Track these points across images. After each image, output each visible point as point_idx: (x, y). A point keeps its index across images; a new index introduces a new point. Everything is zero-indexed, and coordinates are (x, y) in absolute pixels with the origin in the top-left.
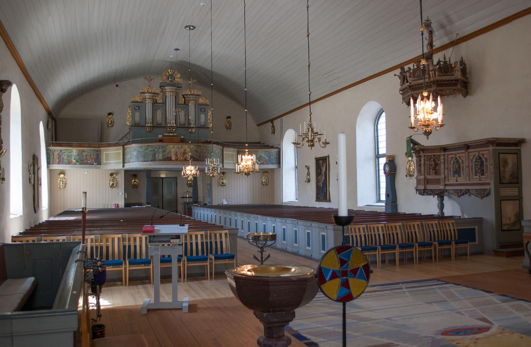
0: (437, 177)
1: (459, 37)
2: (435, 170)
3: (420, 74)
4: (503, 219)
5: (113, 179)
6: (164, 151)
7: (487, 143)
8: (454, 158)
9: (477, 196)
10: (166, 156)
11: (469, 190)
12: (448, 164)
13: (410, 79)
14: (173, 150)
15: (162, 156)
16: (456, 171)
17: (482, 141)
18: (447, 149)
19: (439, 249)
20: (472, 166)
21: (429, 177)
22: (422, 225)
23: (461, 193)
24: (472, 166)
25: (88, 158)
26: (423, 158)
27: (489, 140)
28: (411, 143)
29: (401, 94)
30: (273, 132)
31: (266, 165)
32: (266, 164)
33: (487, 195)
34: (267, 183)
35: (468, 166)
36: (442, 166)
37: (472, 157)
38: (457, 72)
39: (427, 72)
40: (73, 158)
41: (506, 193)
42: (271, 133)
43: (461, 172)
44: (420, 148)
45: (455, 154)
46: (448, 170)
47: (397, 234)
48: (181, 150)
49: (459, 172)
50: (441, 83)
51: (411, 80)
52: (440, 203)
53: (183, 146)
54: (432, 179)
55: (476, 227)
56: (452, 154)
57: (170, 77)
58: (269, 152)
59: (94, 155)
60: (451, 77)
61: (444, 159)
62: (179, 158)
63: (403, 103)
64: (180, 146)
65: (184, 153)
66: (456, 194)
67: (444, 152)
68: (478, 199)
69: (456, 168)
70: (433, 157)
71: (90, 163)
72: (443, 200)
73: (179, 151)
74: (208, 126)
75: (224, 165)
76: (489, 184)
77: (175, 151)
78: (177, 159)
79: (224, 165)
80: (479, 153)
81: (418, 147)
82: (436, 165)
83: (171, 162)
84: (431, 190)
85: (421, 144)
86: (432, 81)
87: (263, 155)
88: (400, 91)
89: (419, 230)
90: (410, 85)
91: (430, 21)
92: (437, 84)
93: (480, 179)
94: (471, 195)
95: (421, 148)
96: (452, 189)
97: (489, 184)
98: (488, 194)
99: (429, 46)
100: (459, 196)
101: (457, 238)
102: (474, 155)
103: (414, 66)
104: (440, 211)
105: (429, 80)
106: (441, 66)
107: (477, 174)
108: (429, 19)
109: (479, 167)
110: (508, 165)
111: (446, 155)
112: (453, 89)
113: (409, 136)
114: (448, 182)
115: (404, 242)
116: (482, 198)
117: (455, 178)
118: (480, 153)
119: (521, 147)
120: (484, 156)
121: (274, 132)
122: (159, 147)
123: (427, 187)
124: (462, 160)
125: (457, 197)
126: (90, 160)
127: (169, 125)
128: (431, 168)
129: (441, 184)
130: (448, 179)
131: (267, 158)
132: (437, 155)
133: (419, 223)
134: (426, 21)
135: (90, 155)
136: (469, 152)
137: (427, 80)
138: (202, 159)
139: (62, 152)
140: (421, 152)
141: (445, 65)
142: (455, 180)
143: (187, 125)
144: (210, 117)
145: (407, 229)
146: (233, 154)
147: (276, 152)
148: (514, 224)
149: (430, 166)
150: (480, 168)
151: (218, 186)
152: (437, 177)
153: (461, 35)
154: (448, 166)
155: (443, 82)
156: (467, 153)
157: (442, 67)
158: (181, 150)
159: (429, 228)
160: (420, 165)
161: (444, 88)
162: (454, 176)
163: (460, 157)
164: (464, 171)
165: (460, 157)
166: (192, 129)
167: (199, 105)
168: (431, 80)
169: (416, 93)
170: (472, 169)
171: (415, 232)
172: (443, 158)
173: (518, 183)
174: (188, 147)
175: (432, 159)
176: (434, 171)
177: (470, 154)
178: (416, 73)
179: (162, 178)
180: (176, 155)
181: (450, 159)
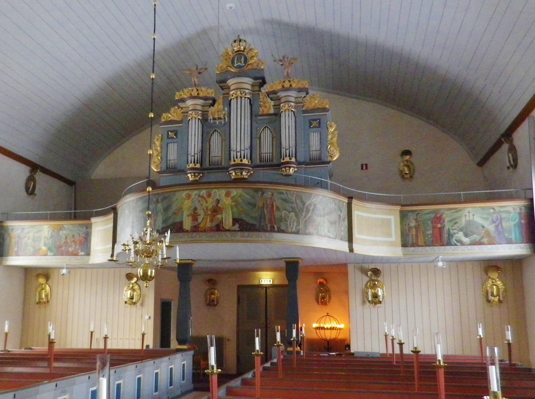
5: (133, 287)
6: (166, 209)
10: (170, 222)
14: (187, 204)
15: (164, 221)
25: (69, 241)
30: (512, 163)
31: (489, 246)
32: (488, 244)
34: (501, 299)
40: (42, 243)
42: (508, 168)
48: (207, 202)
53: (212, 192)
57: (236, 58)
58: (497, 209)
59: (79, 235)
62: (201, 226)
64: (203, 192)
65: (216, 210)
71: (73, 251)
73: (202, 205)
74: (329, 159)
75: (354, 244)
77: (190, 207)
78: (195, 226)
79: (355, 246)
83: (181, 234)
87: (478, 219)
121: (515, 165)
122: (157, 200)
126: (71, 246)
127: (232, 163)
131: (491, 228)
135: (73, 236)
138: (269, 226)
139: (26, 231)
143: (275, 162)
144: (332, 139)
146: (390, 220)
147: (521, 209)
151: (364, 302)
158: (207, 202)
166: (285, 167)
167: (305, 112)
174: (228, 195)
179: (266, 287)
180: (195, 216)
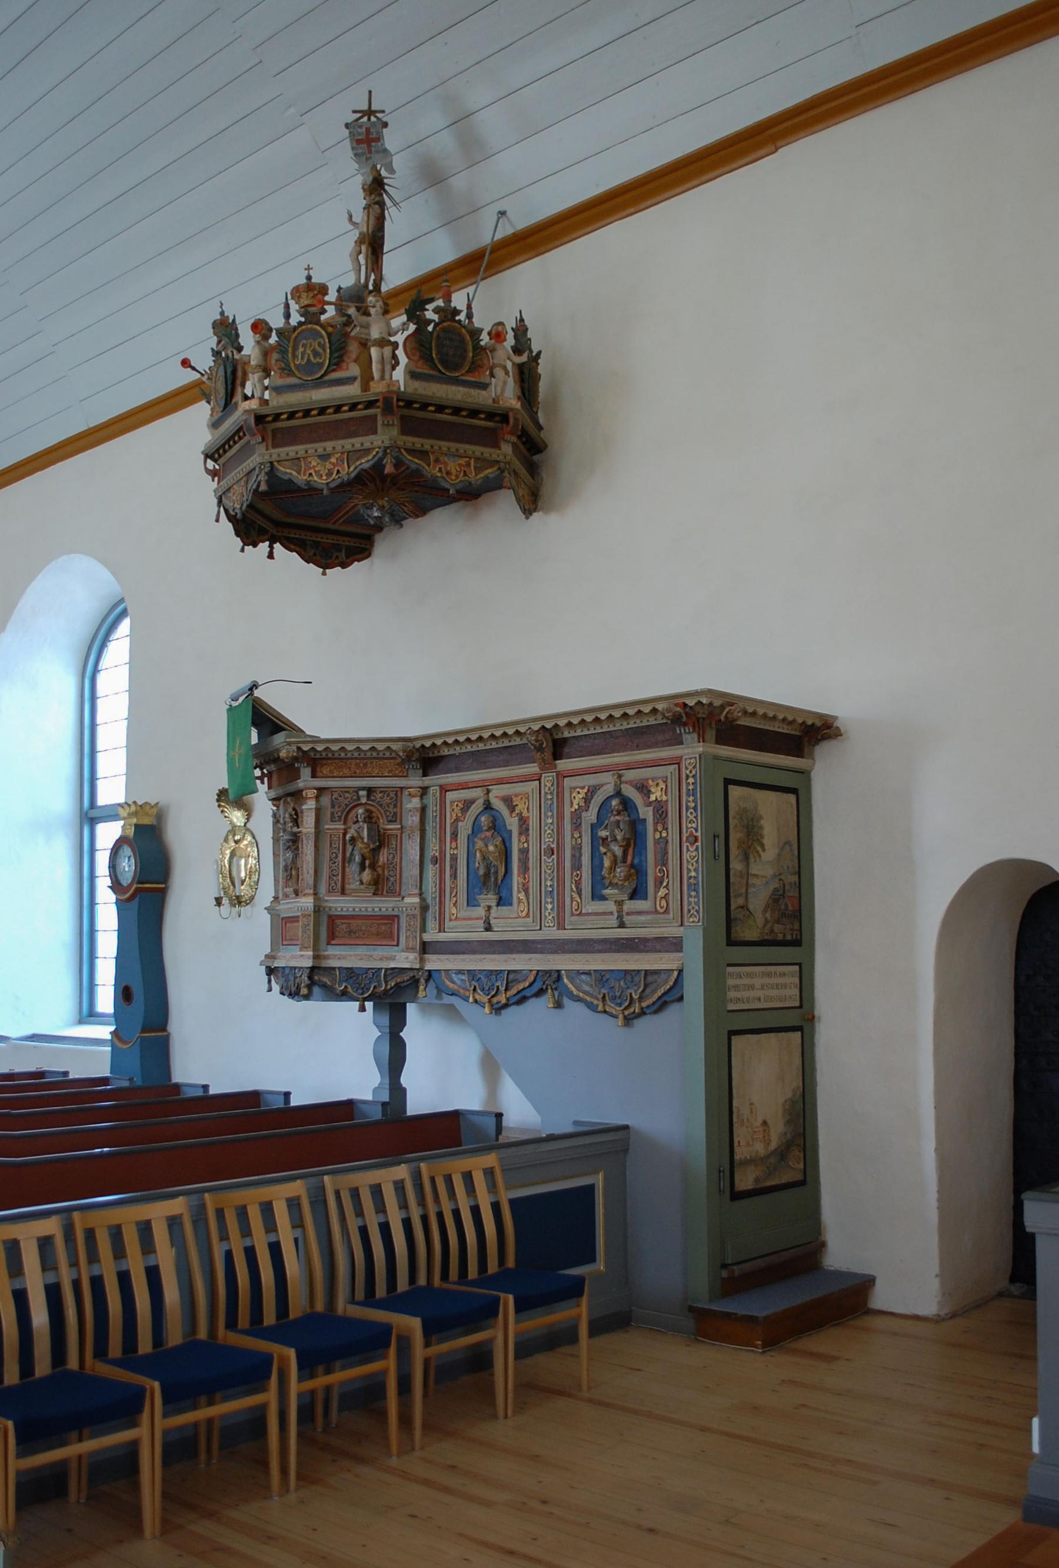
0: (383, 905)
1: (510, 231)
2: (373, 867)
3: (316, 354)
4: (740, 1134)
7: (677, 720)
8: (477, 807)
9: (605, 1012)
11: (559, 978)
12: (442, 841)
13: (266, 382)
16: (487, 875)
17: (647, 709)
18: (440, 759)
19: (427, 1362)
20: (577, 849)
21: (340, 904)
22: (319, 1200)
23: (509, 994)
24: (577, 849)
26: (309, 806)
27: (685, 705)
28: (255, 724)
29: (213, 474)
33: (661, 1006)
35: (554, 846)
36: (412, 849)
37: (578, 799)
38: (499, 372)
39: (353, 348)
41: (746, 994)
43: (516, 879)
44: (299, 748)
45: (486, 786)
46: (442, 872)
47: (153, 1275)
49: (500, 878)
50: (421, 414)
51: (266, 388)
52: (388, 1037)
54: (353, 917)
55: (599, 1180)
56: (464, 786)
60: (474, 392)
61: (423, 810)
63: (217, 520)
66: (485, 999)
67: (425, 774)
68: (608, 1028)
69: (484, 858)
70: (364, 800)
72: (402, 1023)
76: (676, 945)
80: (620, 776)
81: (289, 744)
82: (380, 840)
84: (350, 973)
85: (304, 732)
86: (378, 394)
88: (207, 456)
89: (298, 1232)
90: (265, 411)
91: (378, 115)
92: (403, 418)
93: (620, 917)
94: (566, 1001)
95: (305, 748)
96: (460, 972)
97: (676, 945)
98: (673, 996)
99: (364, 248)
100: (498, 1009)
101: (511, 1263)
102: (592, 792)
103: (287, 316)
104: (387, 1081)
105: (365, 388)
106: (430, 328)
107: (607, 892)
108: (373, 108)
109: (618, 850)
110: (762, 846)
111: (434, 791)
112: (477, 459)
113: (247, 683)
114: (441, 929)
115: (202, 1334)
116: (628, 1021)
117: (481, 912)
118: (623, 779)
119: (811, 756)
120: (649, 793)
123: (326, 957)
124: (520, 814)
125: (487, 1010)
128: (352, 854)
129: (402, 940)
130: (442, 913)
132: (384, 790)
133: (297, 1188)
134: (359, 115)
136: (561, 776)
137: (353, 391)
140: (306, 772)
141: (445, 324)
142: (481, 923)
145: (224, 1237)
148: (782, 1153)
149: (349, 848)
150: (624, 861)
152: (383, 905)
153: (521, 220)
154: (442, 852)
155: (430, 414)
156: (548, 778)
157: (431, 333)
159: (360, 1213)
160: (294, 842)
161: (437, 443)
162: (471, 902)
163: (508, 801)
164: (533, 874)
165: (508, 801)
168: (372, 390)
169: (292, 455)
170: (577, 866)
171: (275, 1249)
172: (419, 806)
173: (797, 943)
175: (361, 811)
176: (367, 871)
177: (568, 782)
178: (295, 349)
181: (457, 810)
